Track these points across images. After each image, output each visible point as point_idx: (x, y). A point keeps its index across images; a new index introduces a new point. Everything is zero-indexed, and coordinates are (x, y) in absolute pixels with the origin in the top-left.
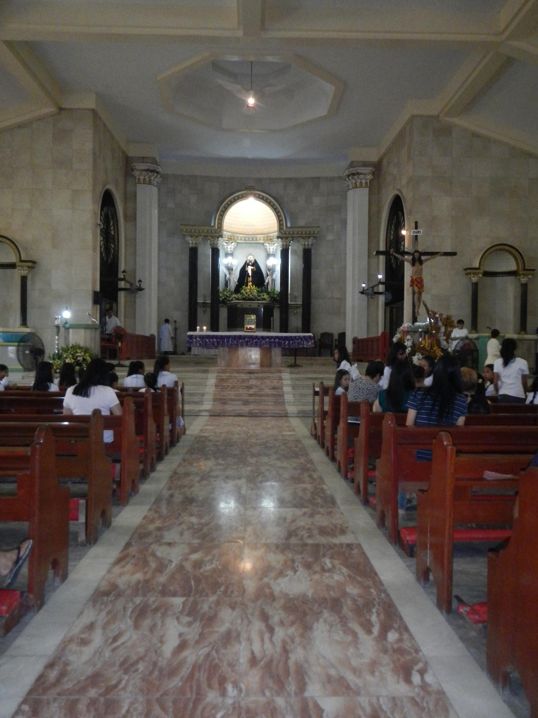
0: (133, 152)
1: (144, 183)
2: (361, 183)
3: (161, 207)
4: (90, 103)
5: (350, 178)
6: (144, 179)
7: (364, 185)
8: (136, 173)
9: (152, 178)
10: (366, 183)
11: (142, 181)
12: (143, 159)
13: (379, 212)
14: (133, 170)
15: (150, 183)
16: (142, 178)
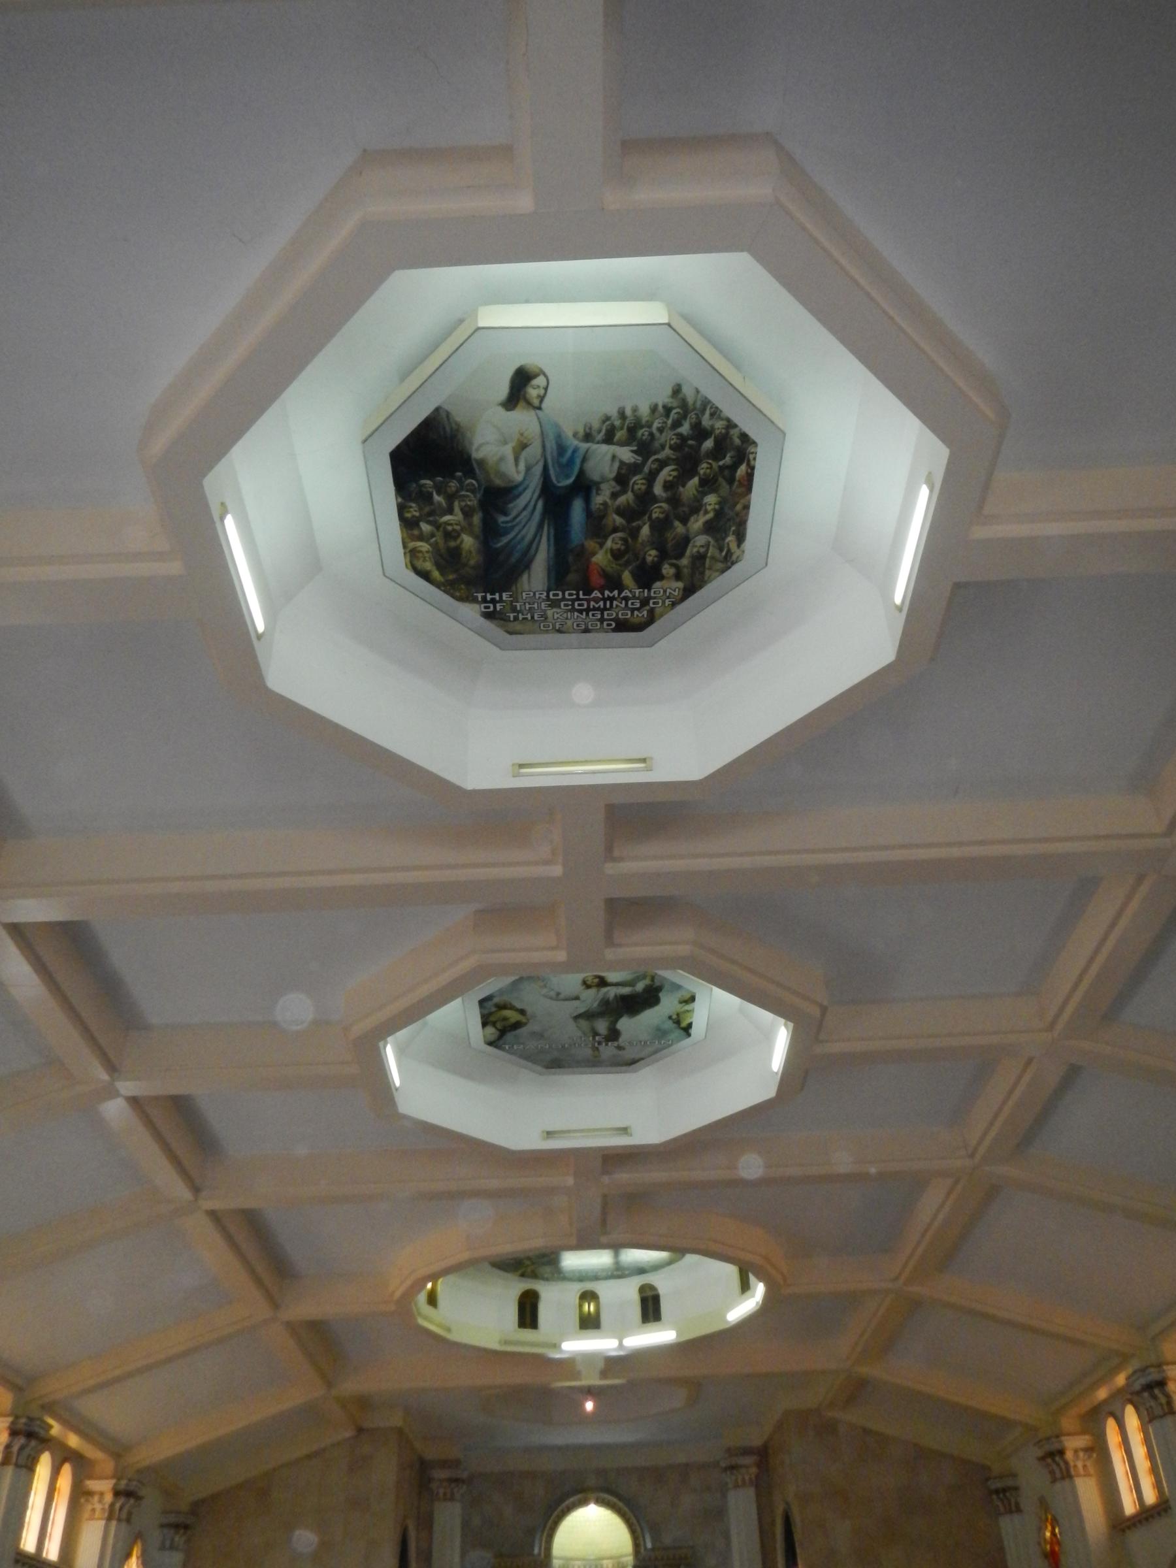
0: (431, 1453)
1: (445, 1499)
2: (743, 1480)
3: (465, 1524)
4: (396, 1420)
5: (728, 1473)
6: (445, 1494)
7: (747, 1481)
8: (434, 1485)
9: (455, 1490)
10: (750, 1479)
11: (441, 1495)
12: (445, 1464)
13: (773, 1523)
14: (430, 1480)
15: (452, 1499)
16: (441, 1491)
